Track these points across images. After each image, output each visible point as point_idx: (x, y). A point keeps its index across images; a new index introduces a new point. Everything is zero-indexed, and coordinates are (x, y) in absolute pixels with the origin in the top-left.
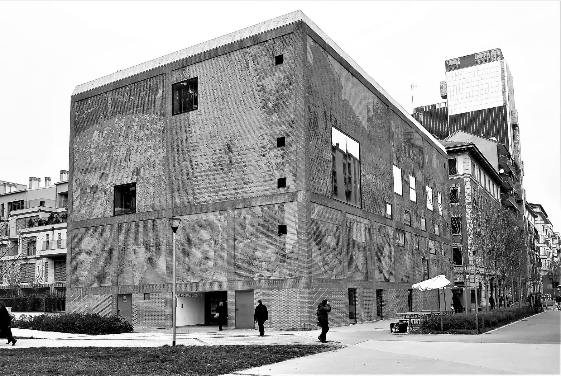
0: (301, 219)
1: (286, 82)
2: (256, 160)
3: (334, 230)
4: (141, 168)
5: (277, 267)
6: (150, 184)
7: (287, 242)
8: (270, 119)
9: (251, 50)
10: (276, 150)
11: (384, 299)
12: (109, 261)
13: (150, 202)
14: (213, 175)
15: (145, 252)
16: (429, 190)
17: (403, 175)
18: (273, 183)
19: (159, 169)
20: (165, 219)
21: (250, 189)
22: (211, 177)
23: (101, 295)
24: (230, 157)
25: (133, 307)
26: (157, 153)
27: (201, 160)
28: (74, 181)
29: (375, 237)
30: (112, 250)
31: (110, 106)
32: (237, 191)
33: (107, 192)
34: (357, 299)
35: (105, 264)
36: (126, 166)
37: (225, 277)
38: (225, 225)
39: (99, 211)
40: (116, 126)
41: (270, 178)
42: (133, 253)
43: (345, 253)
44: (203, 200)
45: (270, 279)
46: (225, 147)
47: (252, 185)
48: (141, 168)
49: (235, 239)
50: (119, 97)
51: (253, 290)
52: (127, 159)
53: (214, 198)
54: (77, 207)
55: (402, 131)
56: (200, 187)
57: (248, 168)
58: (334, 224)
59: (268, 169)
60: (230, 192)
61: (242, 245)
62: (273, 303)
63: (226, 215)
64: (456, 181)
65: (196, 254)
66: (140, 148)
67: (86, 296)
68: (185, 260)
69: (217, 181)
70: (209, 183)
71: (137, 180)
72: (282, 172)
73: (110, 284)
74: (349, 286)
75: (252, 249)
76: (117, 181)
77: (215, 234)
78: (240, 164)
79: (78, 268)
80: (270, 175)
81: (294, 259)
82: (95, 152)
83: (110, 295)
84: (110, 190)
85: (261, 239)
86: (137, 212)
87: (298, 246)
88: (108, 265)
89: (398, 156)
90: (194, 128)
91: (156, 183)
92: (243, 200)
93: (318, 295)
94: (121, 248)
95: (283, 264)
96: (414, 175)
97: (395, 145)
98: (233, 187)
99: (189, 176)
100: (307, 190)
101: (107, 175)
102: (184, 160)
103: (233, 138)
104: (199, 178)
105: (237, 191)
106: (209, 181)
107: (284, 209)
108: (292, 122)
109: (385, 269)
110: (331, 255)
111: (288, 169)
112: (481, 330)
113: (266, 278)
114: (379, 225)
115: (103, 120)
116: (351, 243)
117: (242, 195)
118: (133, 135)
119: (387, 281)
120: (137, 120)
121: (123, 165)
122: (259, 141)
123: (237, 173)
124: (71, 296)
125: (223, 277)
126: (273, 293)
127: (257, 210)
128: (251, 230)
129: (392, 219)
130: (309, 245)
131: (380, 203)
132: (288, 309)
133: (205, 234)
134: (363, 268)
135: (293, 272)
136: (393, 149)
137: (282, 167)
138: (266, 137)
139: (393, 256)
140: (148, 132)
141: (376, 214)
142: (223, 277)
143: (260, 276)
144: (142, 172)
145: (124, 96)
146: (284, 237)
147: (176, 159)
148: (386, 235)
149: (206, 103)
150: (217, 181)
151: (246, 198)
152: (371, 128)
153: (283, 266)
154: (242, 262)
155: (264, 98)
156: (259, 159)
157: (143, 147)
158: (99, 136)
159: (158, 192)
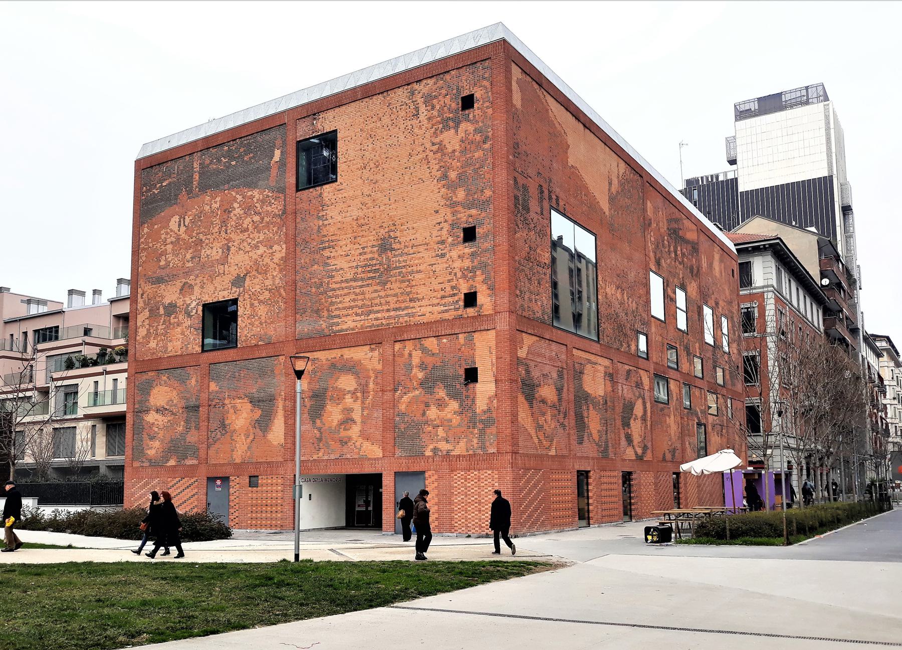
0: (501, 358)
1: (478, 137)
2: (429, 263)
3: (555, 375)
4: (245, 275)
5: (463, 436)
6: (260, 302)
7: (478, 395)
8: (451, 197)
9: (422, 87)
10: (461, 247)
11: (634, 488)
12: (193, 424)
13: (259, 330)
14: (361, 287)
15: (252, 411)
16: (707, 312)
17: (665, 288)
18: (456, 299)
19: (275, 278)
20: (283, 357)
21: (420, 310)
22: (357, 291)
23: (180, 479)
24: (388, 258)
25: (232, 498)
26: (271, 251)
27: (341, 263)
28: (139, 296)
29: (620, 388)
30: (198, 407)
31: (196, 177)
32: (398, 313)
33: (192, 314)
34: (590, 487)
35: (188, 429)
36: (221, 272)
38: (379, 367)
39: (178, 344)
40: (207, 208)
41: (451, 292)
42: (232, 411)
43: (572, 413)
44: (344, 327)
45: (451, 454)
46: (380, 242)
47: (423, 303)
48: (245, 275)
49: (395, 390)
50: (211, 162)
51: (423, 473)
52: (224, 261)
53: (362, 323)
54: (143, 338)
55: (665, 217)
56: (340, 306)
57: (418, 276)
58: (554, 366)
59: (450, 278)
60: (387, 315)
61: (405, 398)
62: (456, 493)
63: (381, 351)
64: (751, 298)
65: (333, 414)
66: (245, 244)
67: (157, 481)
68: (314, 422)
69: (367, 296)
70: (354, 300)
71: (239, 295)
72: (471, 282)
73: (195, 462)
74: (577, 467)
75: (422, 406)
76: (207, 296)
77: (363, 382)
78: (404, 270)
79: (145, 436)
80: (451, 287)
81: (488, 423)
82: (172, 250)
83: (195, 479)
84: (197, 311)
85: (436, 390)
86: (239, 346)
87: (496, 401)
88: (193, 431)
89: (657, 258)
90: (332, 213)
91: (269, 299)
92: (408, 327)
93: (528, 482)
94: (214, 403)
95: (471, 430)
96: (683, 288)
97: (653, 239)
98: (392, 306)
99: (322, 289)
100: (511, 312)
101: (191, 287)
102: (314, 262)
103: (393, 228)
104: (338, 292)
105: (398, 313)
106: (353, 296)
107: (474, 342)
108: (487, 201)
109: (636, 439)
110: (549, 417)
111: (480, 278)
112: (791, 538)
113: (445, 453)
114: (627, 367)
115: (186, 197)
116: (582, 398)
117: (406, 318)
118: (233, 223)
119: (640, 458)
120: (239, 198)
121: (217, 270)
122: (435, 233)
123: (398, 284)
124: (133, 481)
125: (376, 451)
126: (455, 477)
127: (431, 343)
128: (420, 375)
129: (647, 359)
130: (514, 400)
131: (629, 332)
132: (480, 503)
133: (347, 382)
134: (600, 437)
135: (488, 444)
136: (651, 247)
137: (471, 274)
138: (446, 226)
139: (649, 419)
140: (256, 218)
141: (622, 350)
142: (376, 451)
143: (435, 450)
144: (248, 282)
145: (219, 161)
146: (474, 387)
147: (302, 261)
148: (639, 385)
149: (349, 171)
150: (367, 296)
151: (413, 324)
152: (615, 211)
153: (472, 433)
154: (406, 426)
155: (442, 164)
156: (433, 261)
157: (249, 242)
158: (179, 225)
159: (273, 313)
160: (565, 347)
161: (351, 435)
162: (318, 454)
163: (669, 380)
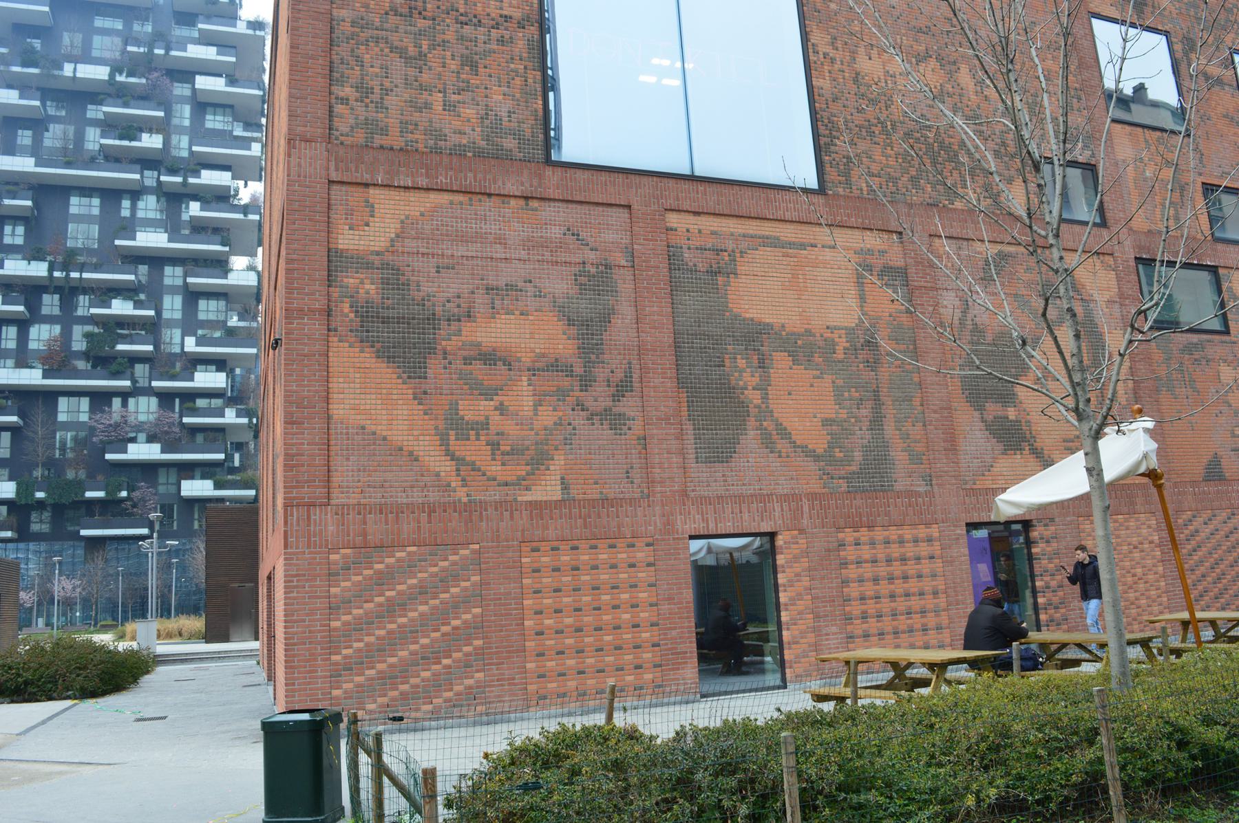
3: (560, 285)
34: (781, 578)
160: (624, 214)
163: (1221, 271)
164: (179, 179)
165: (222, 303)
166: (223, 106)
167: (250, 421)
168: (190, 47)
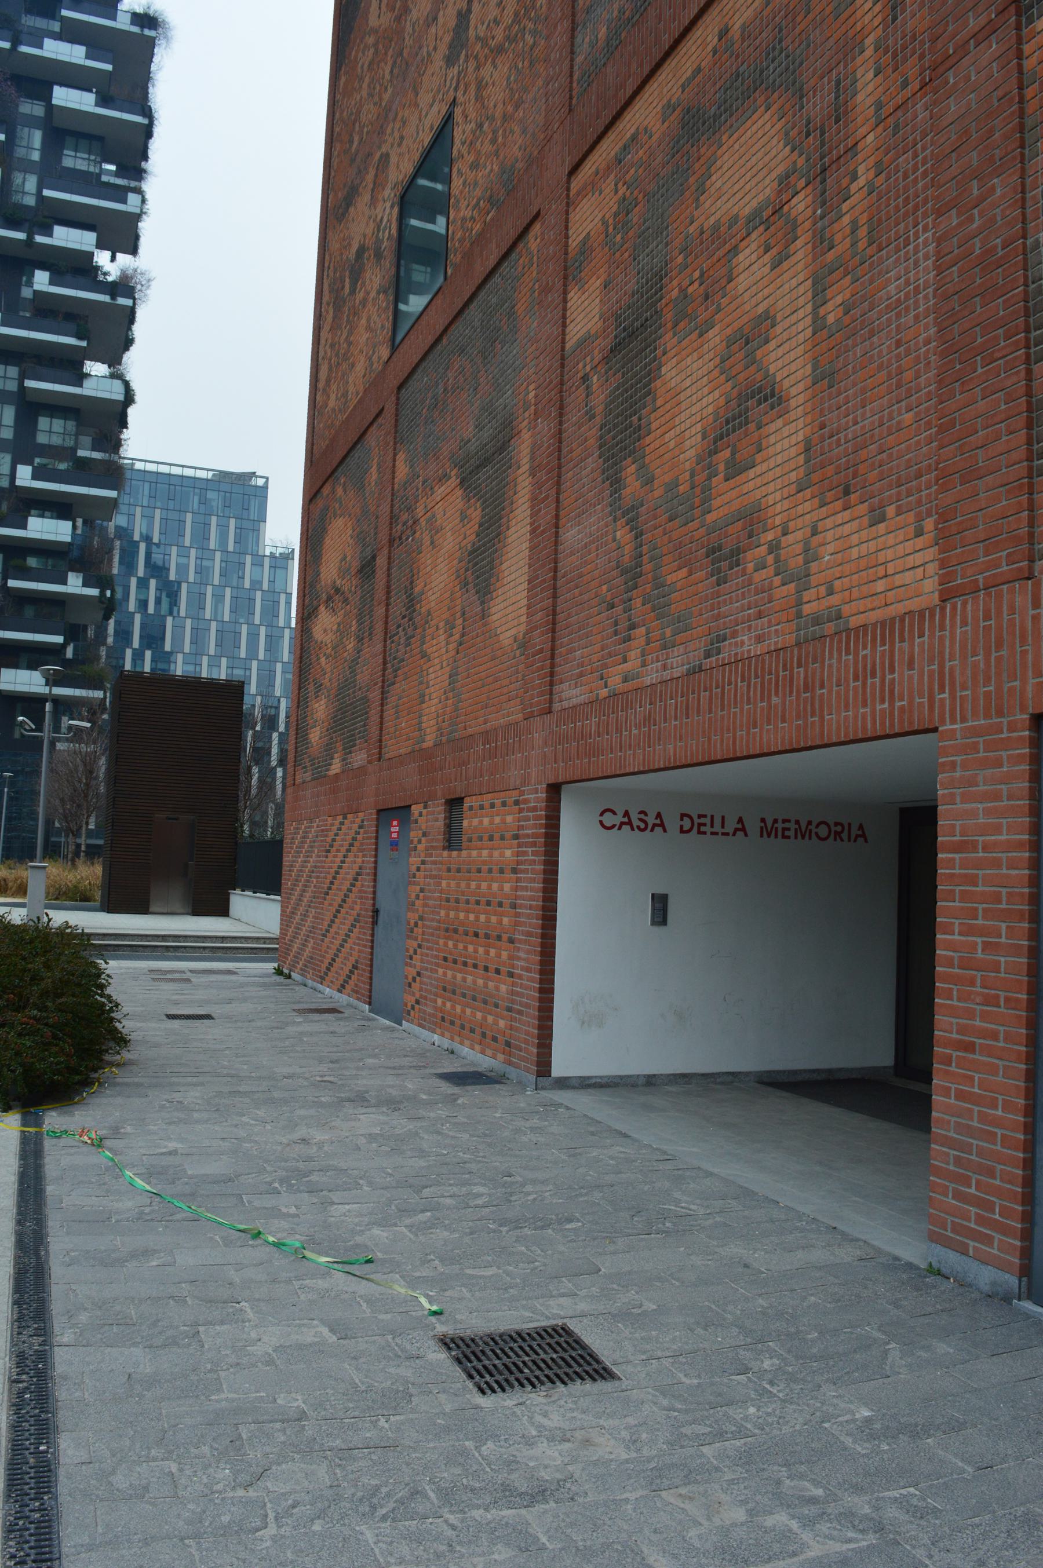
37: (918, 558)
68: (616, 483)
161: (758, 494)
162: (625, 661)
164: (21, 236)
165: (71, 425)
166: (89, 137)
167: (103, 593)
168: (48, 43)
